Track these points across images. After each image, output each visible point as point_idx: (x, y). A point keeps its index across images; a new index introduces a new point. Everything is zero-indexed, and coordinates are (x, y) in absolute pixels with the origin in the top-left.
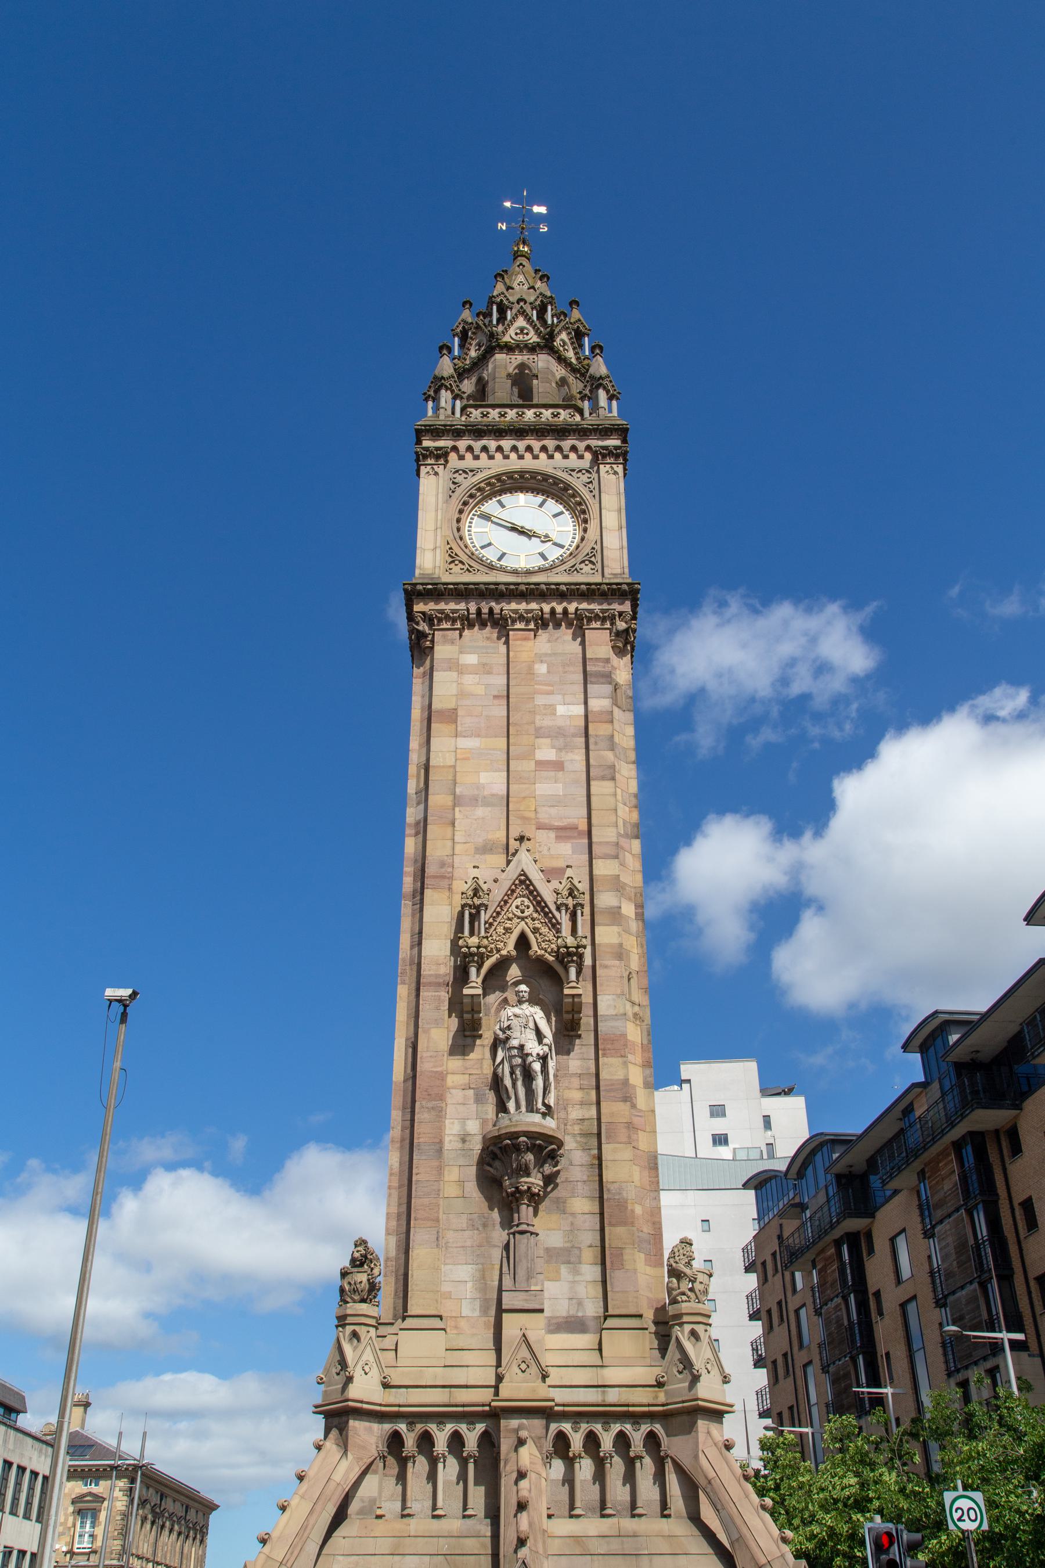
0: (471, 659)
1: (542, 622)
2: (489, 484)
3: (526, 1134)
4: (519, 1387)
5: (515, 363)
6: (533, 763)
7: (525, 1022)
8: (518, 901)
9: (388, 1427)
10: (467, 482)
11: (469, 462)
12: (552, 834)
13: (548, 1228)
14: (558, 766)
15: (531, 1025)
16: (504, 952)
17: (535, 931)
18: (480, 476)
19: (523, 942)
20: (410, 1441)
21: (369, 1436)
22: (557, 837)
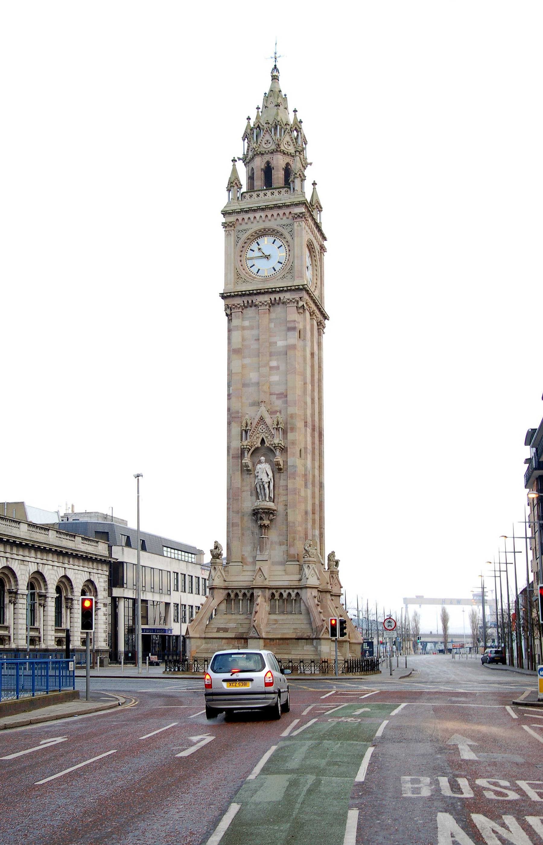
0: (246, 323)
1: (273, 304)
2: (256, 233)
3: (262, 509)
4: (259, 582)
5: (265, 161)
6: (268, 369)
7: (264, 470)
8: (261, 427)
9: (227, 591)
10: (244, 237)
11: (244, 227)
12: (275, 396)
13: (273, 535)
14: (278, 368)
15: (265, 471)
16: (256, 446)
17: (267, 437)
18: (249, 233)
19: (263, 441)
20: (232, 596)
21: (221, 595)
22: (277, 398)
